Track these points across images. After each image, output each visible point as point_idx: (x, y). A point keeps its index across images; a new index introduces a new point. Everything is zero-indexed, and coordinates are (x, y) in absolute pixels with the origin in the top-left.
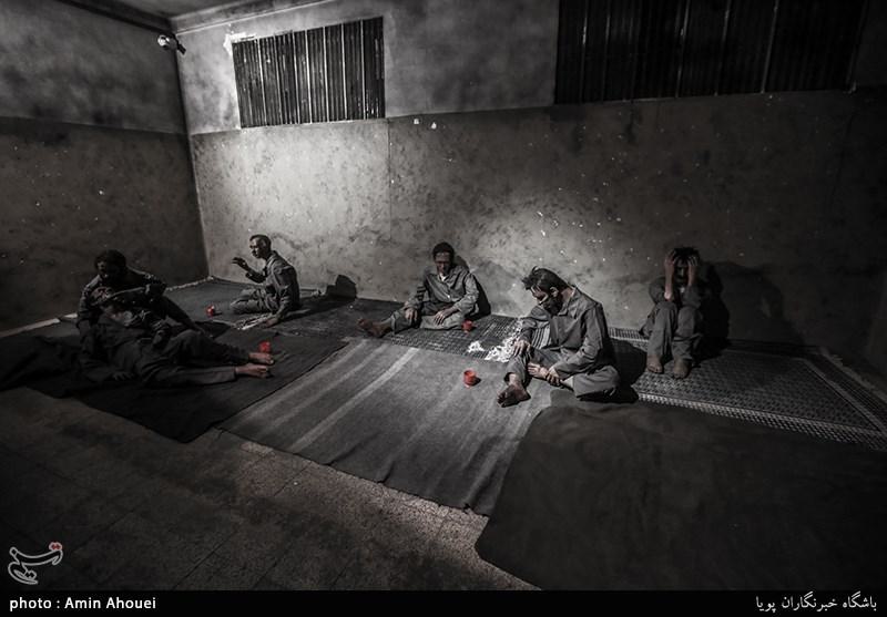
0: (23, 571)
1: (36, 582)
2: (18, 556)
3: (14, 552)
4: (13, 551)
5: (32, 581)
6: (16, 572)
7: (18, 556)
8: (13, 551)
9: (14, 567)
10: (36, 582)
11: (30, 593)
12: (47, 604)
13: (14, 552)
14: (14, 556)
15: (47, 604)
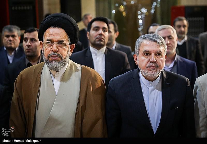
0: (5, 133)
1: (8, 136)
2: (4, 130)
3: (3, 129)
4: (3, 129)
5: (7, 136)
6: (3, 133)
7: (4, 130)
8: (3, 129)
9: (3, 132)
10: (8, 136)
11: (6, 138)
12: (10, 141)
13: (3, 129)
14: (3, 130)
15: (10, 141)
